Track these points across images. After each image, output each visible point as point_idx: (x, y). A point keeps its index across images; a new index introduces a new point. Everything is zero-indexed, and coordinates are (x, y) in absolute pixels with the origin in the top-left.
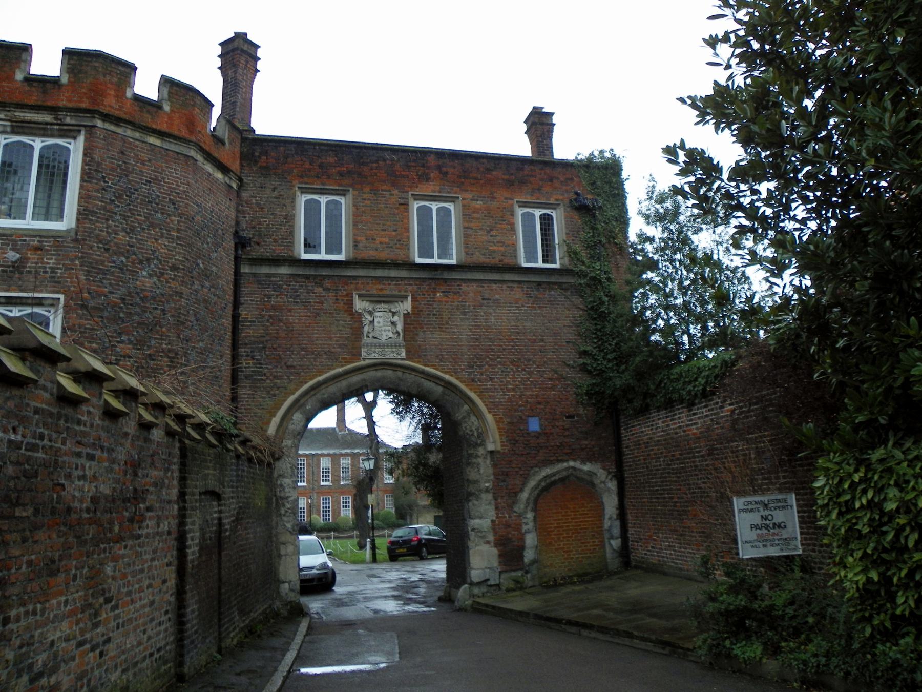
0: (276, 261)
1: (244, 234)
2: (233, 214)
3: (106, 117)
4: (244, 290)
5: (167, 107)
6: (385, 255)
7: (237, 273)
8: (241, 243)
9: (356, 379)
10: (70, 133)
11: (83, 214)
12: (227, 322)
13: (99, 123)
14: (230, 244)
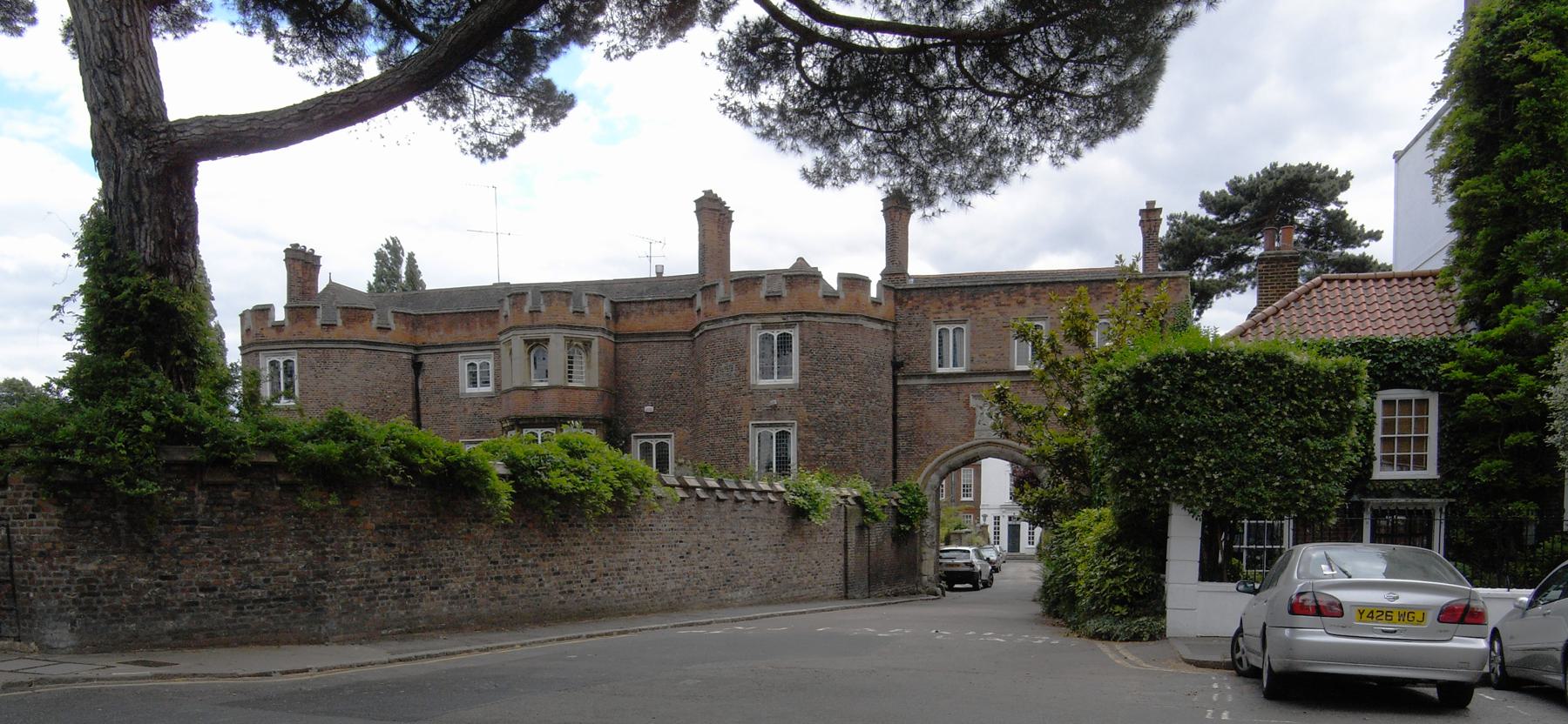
0: (920, 376)
1: (899, 359)
2: (890, 347)
3: (808, 314)
4: (900, 396)
5: (842, 296)
6: (991, 366)
7: (895, 387)
8: (897, 366)
9: (971, 453)
10: (789, 325)
11: (803, 374)
12: (889, 421)
13: (805, 318)
14: (889, 369)
